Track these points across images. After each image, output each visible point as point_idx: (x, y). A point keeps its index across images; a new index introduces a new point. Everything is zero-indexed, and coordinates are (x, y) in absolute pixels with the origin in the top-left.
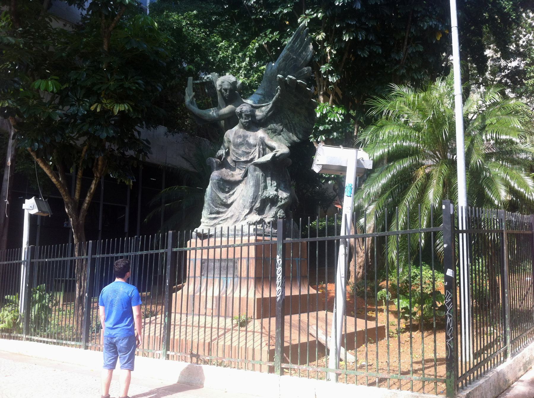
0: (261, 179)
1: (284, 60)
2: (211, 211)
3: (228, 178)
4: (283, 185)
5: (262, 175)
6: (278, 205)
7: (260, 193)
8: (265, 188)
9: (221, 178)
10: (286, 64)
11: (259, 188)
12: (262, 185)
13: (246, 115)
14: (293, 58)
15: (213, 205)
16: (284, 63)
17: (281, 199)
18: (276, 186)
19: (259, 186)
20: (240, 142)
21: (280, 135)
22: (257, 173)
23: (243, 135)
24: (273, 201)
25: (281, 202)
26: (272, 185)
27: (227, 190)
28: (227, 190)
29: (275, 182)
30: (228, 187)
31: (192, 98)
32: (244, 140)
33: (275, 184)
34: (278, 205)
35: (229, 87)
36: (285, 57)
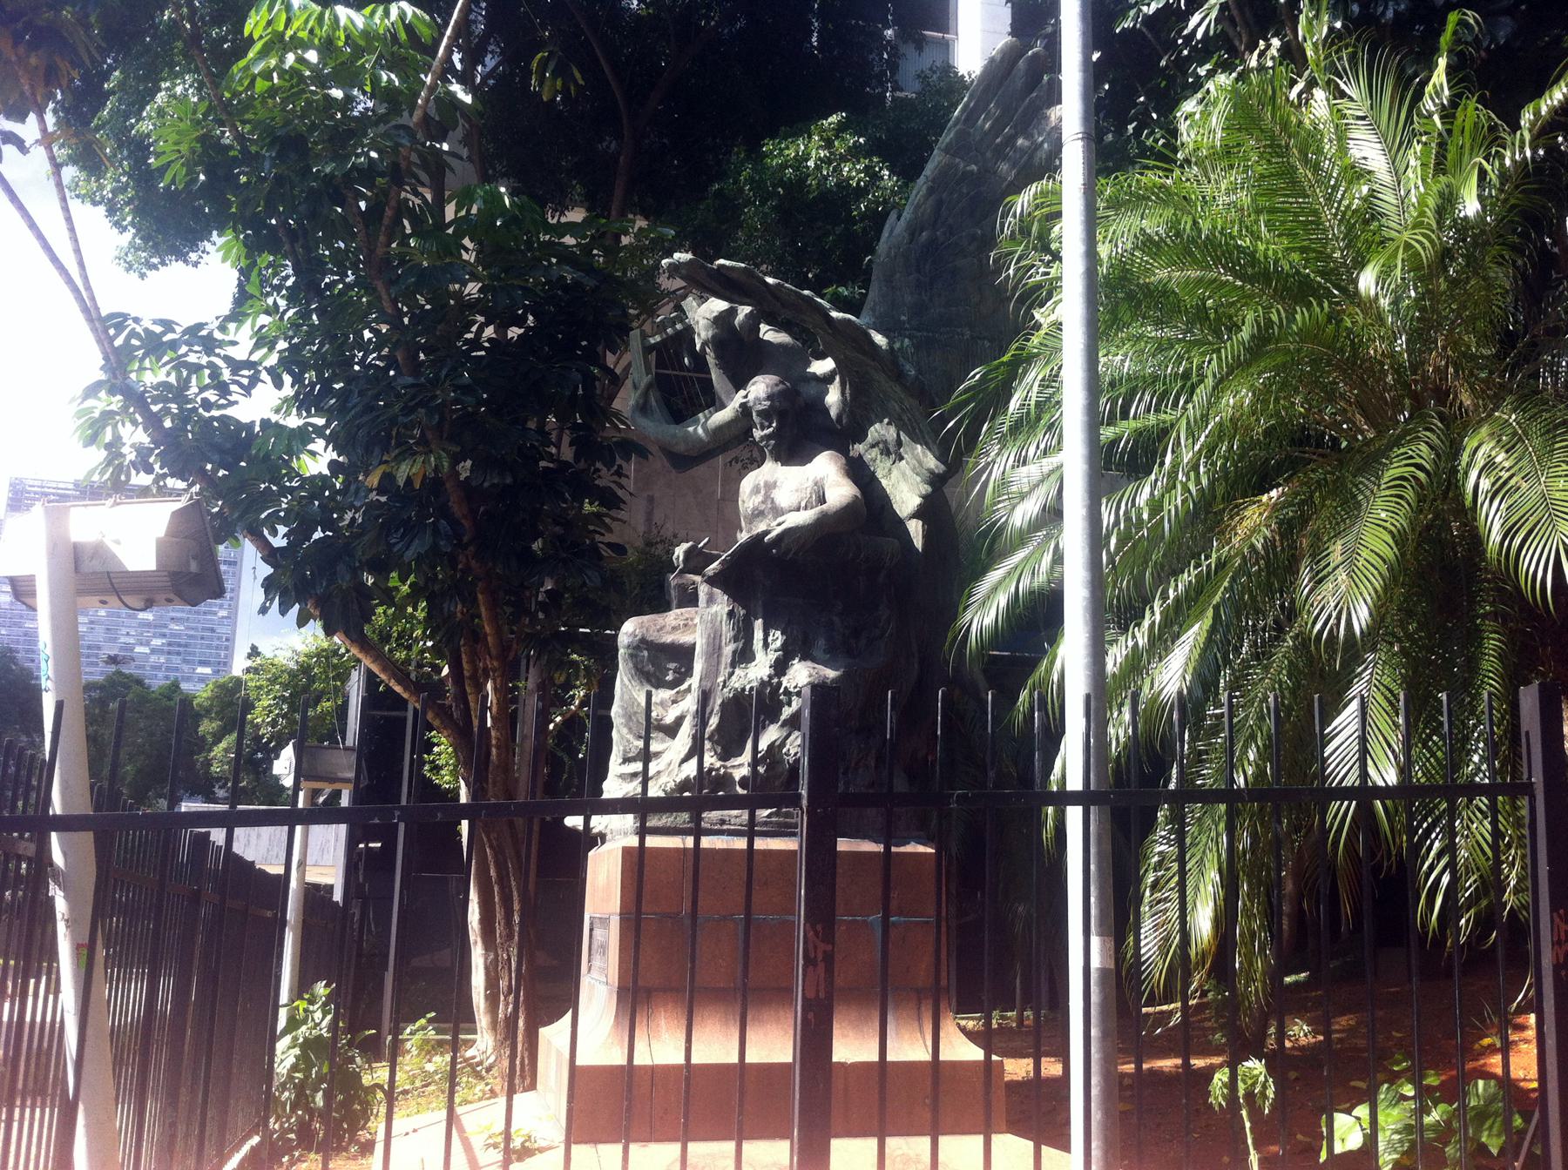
0: (727, 631)
1: (931, 191)
2: (625, 751)
3: (668, 639)
4: (821, 642)
5: (731, 614)
6: (783, 717)
7: (721, 679)
8: (744, 656)
9: (643, 641)
10: (940, 203)
11: (719, 663)
12: (728, 650)
13: (760, 413)
14: (966, 175)
15: (630, 729)
16: (931, 201)
17: (787, 692)
18: (784, 647)
19: (719, 656)
20: (754, 509)
21: (901, 458)
22: (715, 608)
23: (766, 484)
24: (766, 702)
25: (789, 704)
26: (766, 645)
27: (669, 677)
28: (669, 677)
29: (778, 633)
30: (672, 666)
31: (646, 394)
32: (767, 497)
33: (778, 643)
34: (783, 717)
35: (710, 333)
36: (933, 181)
